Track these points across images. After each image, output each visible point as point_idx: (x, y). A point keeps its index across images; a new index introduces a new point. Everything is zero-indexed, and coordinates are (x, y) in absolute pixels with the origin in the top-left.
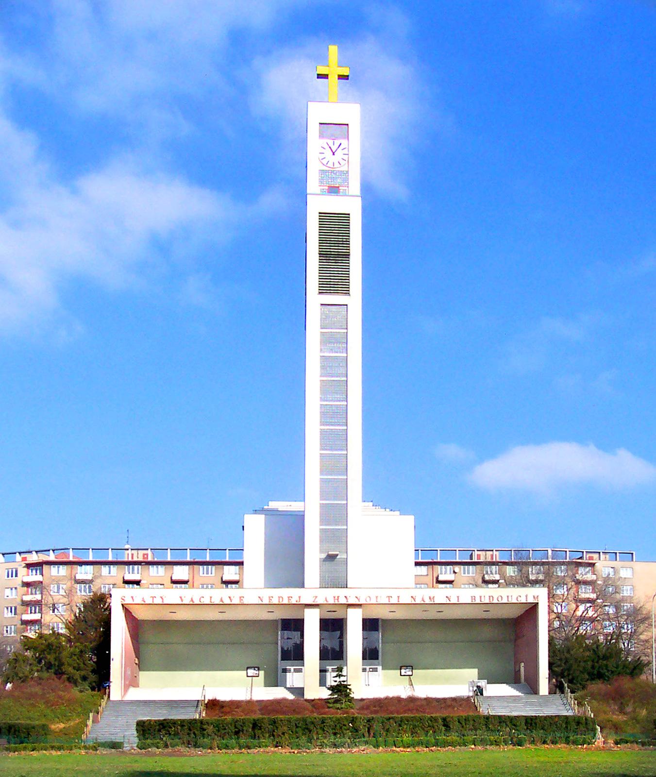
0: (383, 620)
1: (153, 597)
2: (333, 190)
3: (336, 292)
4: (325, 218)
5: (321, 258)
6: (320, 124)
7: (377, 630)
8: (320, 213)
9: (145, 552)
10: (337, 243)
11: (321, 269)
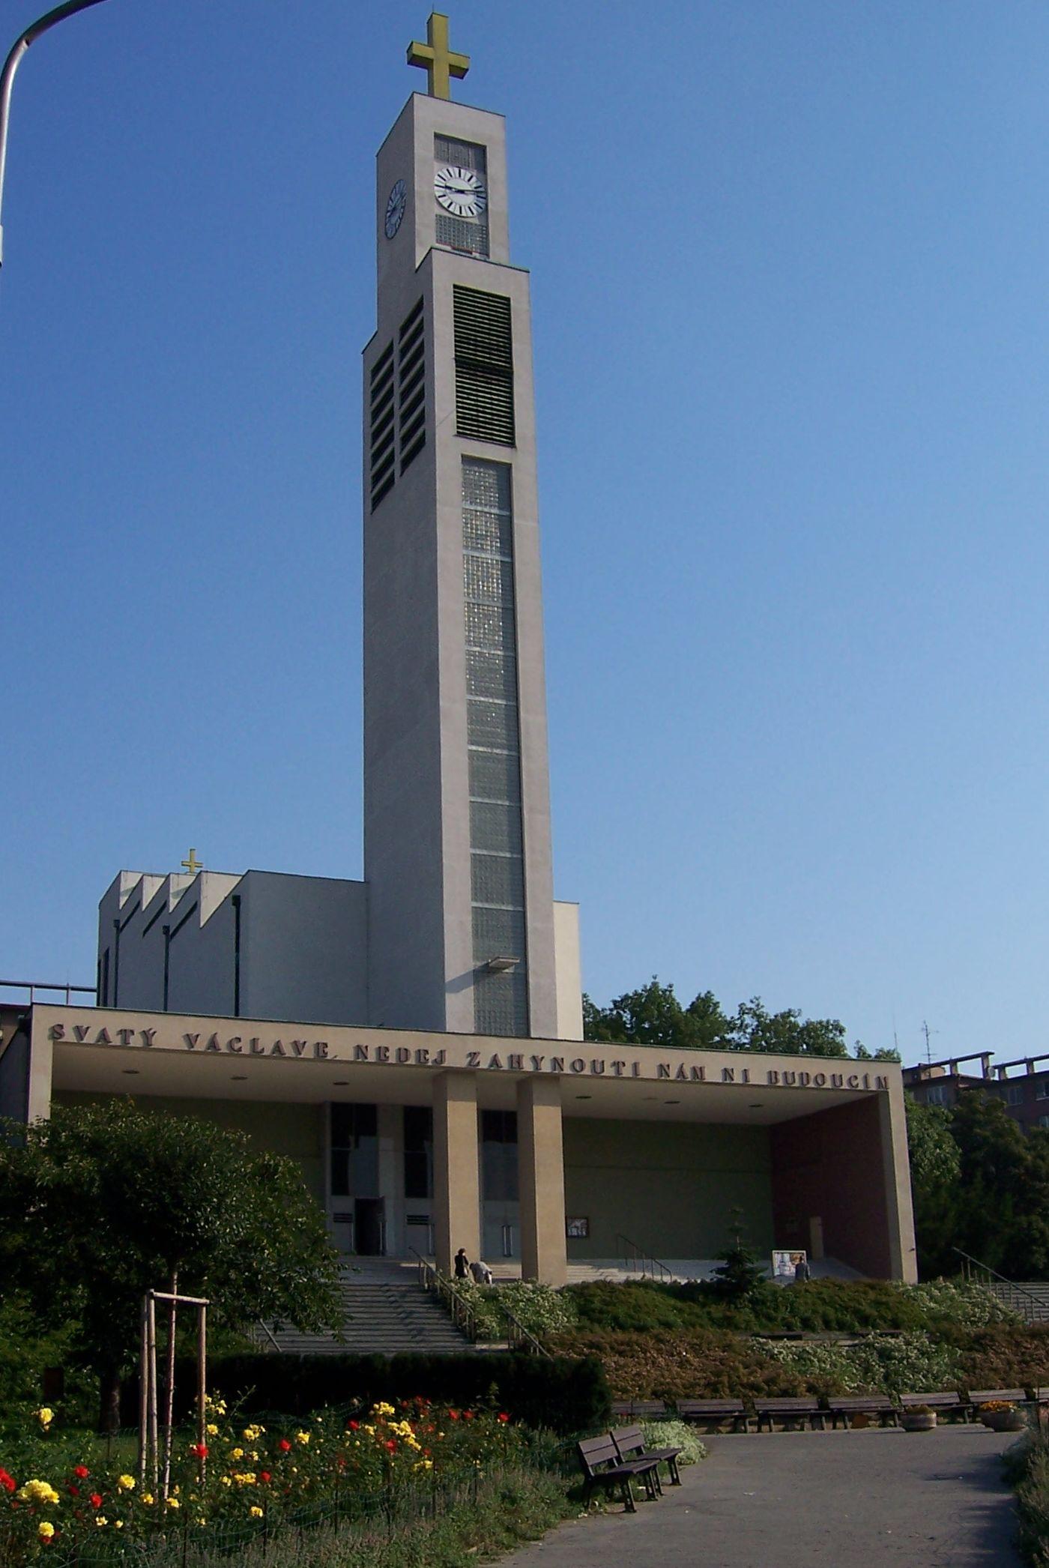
3: (490, 439)
4: (463, 295)
5: (459, 369)
6: (437, 136)
8: (455, 286)
10: (489, 348)
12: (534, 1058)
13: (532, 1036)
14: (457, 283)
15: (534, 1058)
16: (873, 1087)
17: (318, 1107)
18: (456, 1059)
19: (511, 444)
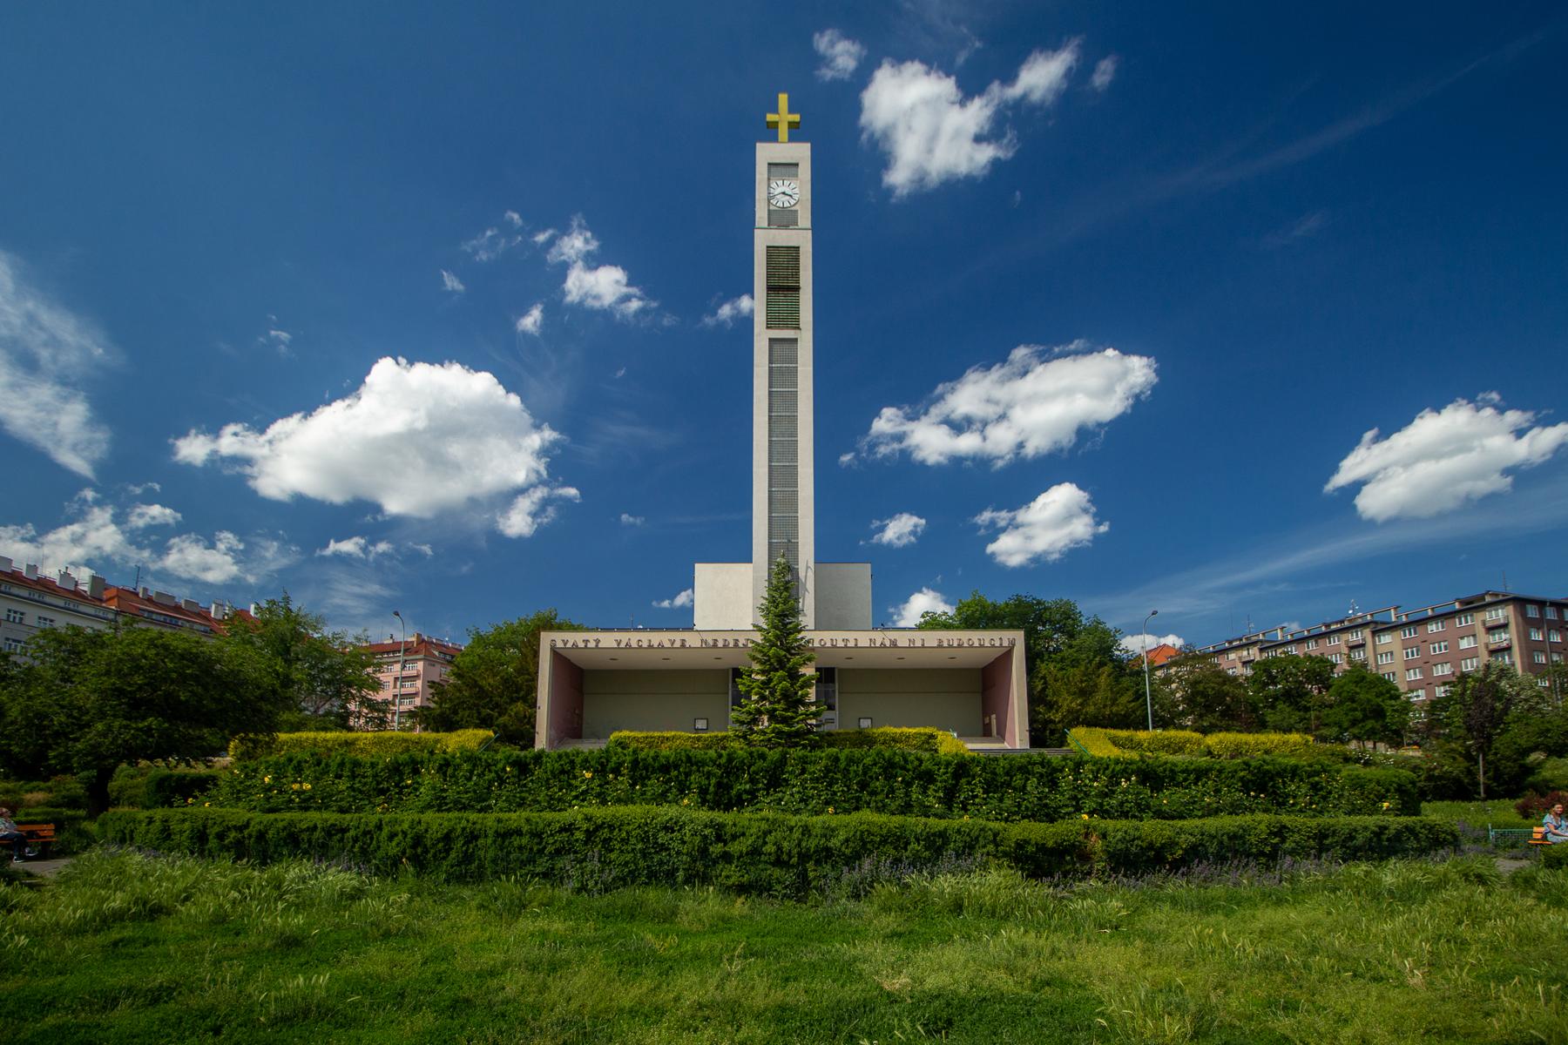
0: (841, 670)
1: (586, 641)
4: (772, 251)
6: (769, 164)
7: (833, 682)
19: (799, 328)
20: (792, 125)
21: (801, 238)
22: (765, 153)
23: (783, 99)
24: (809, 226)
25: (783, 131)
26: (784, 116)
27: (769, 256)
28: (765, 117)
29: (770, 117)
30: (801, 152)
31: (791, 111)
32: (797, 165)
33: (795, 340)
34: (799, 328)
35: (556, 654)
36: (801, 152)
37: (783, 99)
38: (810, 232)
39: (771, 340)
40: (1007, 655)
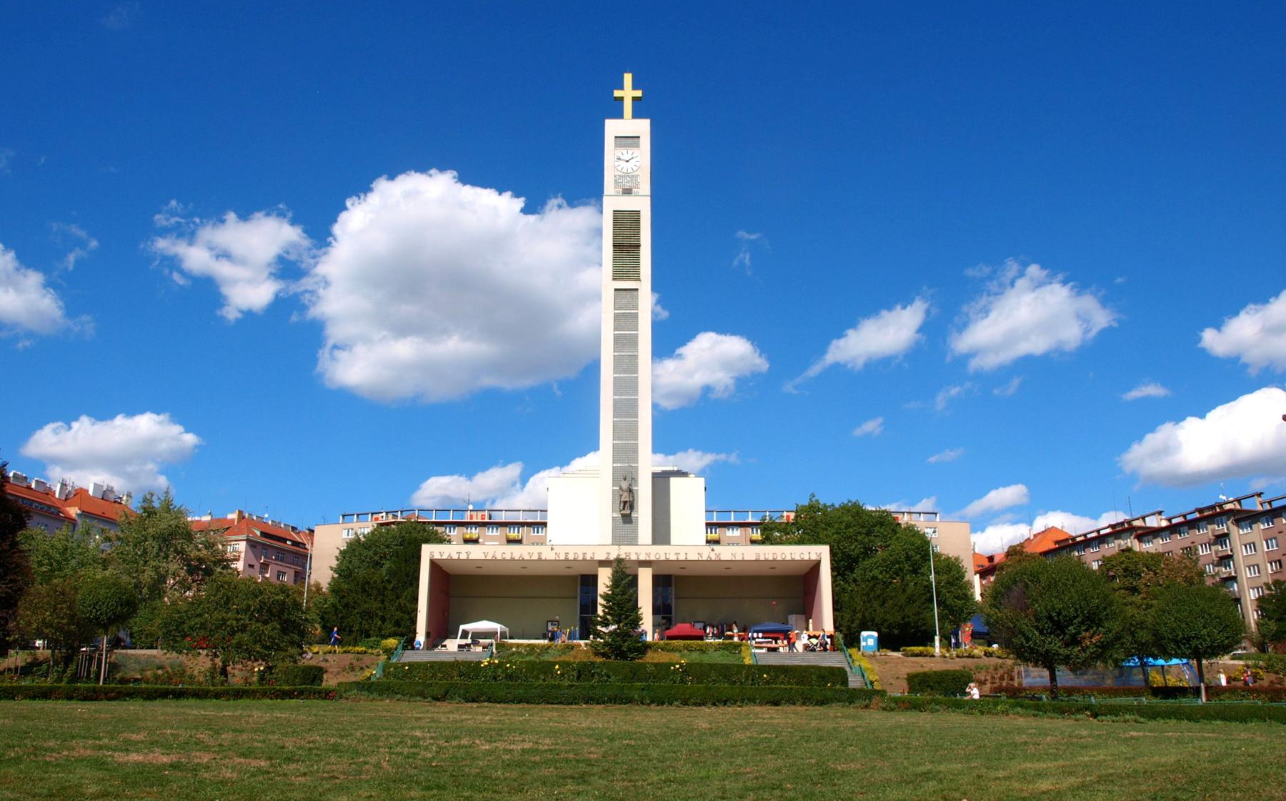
2: (627, 192)
3: (629, 278)
6: (616, 137)
9: (483, 513)
10: (630, 237)
11: (615, 259)
12: (636, 554)
13: (639, 543)
14: (615, 209)
15: (636, 554)
16: (814, 557)
17: (576, 576)
18: (601, 556)
19: (639, 280)
20: (634, 99)
21: (642, 203)
22: (613, 128)
23: (628, 78)
24: (649, 194)
25: (628, 107)
26: (628, 92)
27: (615, 219)
28: (613, 93)
29: (617, 93)
30: (642, 127)
31: (635, 87)
32: (639, 137)
33: (637, 290)
34: (639, 280)
35: (434, 564)
36: (642, 127)
37: (628, 78)
38: (649, 198)
39: (616, 290)
40: (816, 566)
